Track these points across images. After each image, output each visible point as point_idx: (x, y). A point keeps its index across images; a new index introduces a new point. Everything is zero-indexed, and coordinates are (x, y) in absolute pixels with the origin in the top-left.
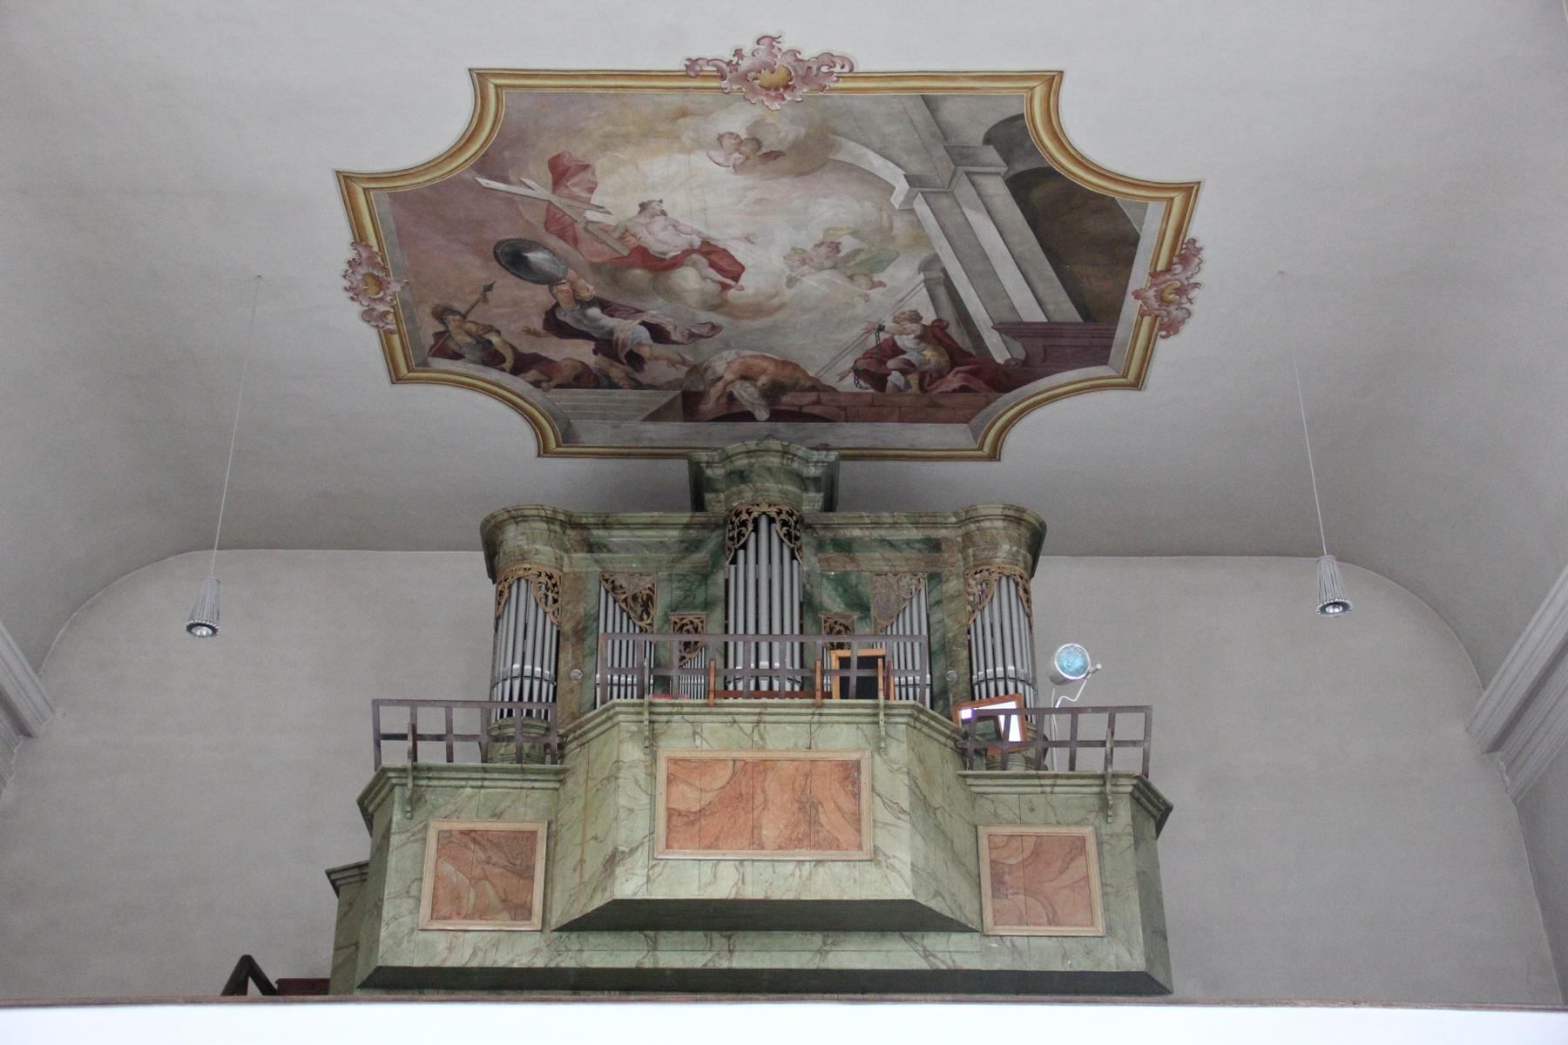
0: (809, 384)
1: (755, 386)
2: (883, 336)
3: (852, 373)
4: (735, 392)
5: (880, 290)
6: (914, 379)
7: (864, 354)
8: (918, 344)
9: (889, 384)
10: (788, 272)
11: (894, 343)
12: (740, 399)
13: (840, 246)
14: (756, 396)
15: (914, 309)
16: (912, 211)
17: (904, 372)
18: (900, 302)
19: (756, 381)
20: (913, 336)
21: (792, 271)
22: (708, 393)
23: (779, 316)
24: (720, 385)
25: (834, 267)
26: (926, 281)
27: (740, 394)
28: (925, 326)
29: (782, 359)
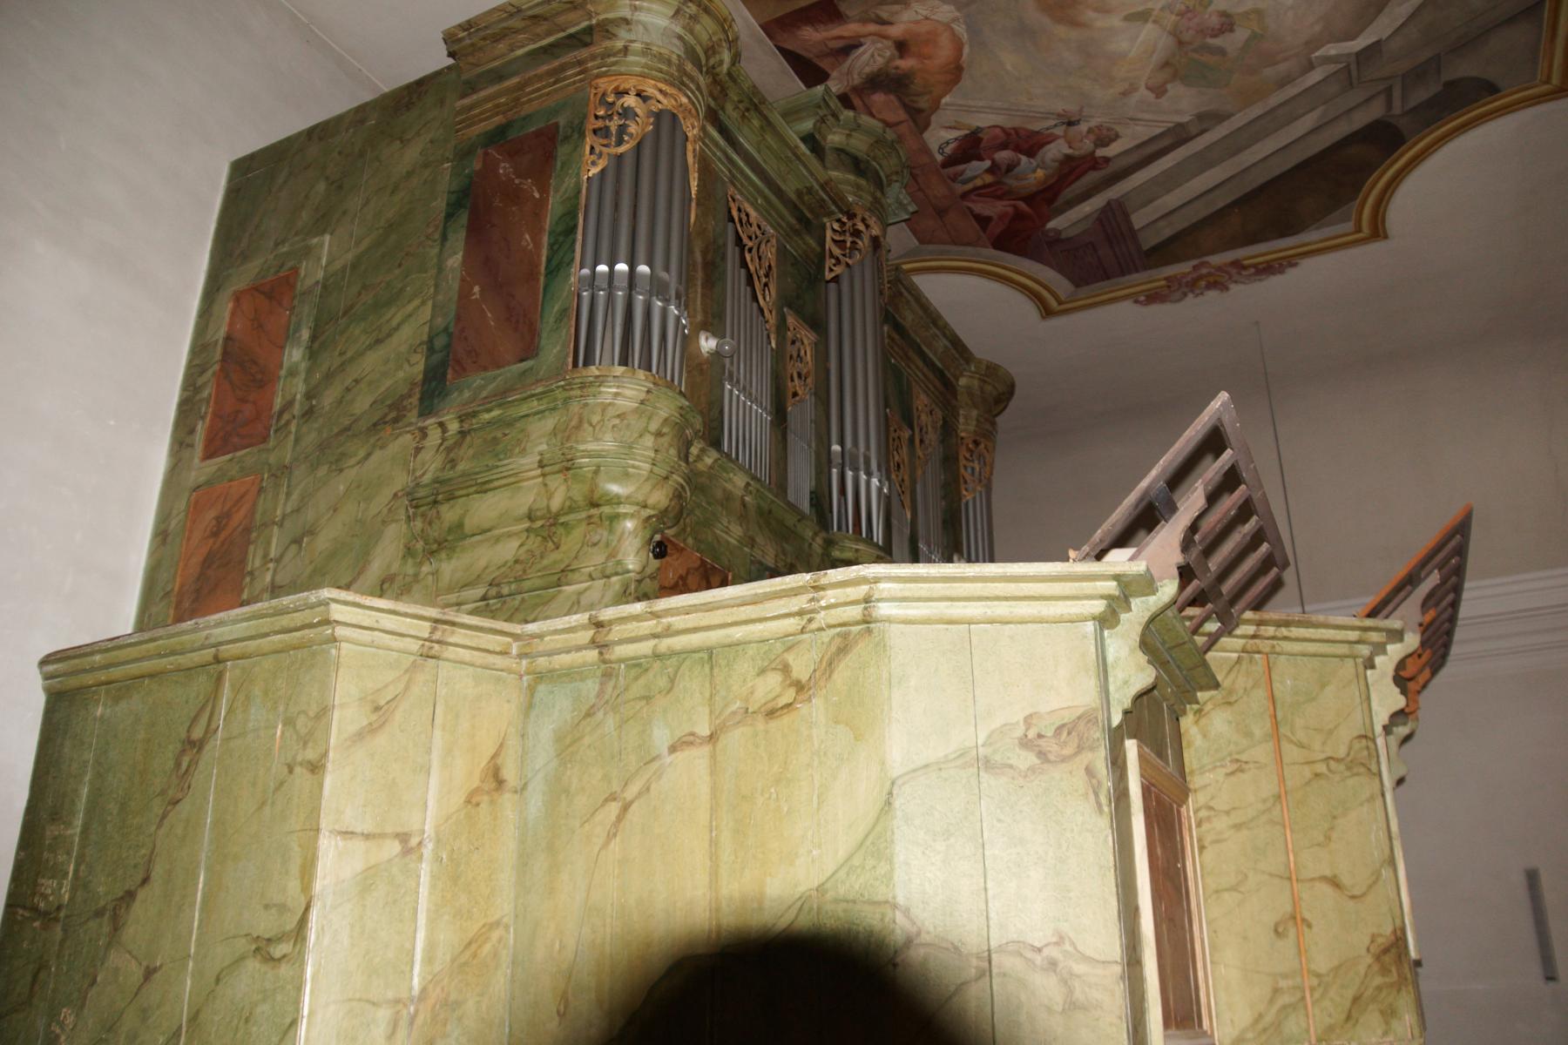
0: (923, 103)
1: (891, 59)
2: (1059, 131)
3: (968, 132)
4: (861, 49)
5: (1150, 96)
6: (989, 179)
7: (1014, 129)
8: (1053, 161)
9: (961, 167)
10: (1159, 6)
11: (1049, 143)
12: (852, 57)
13: (1227, 34)
14: (867, 70)
15: (1120, 134)
16: (1311, 66)
17: (990, 171)
18: (1131, 119)
19: (901, 57)
20: (1069, 151)
21: (1162, 9)
22: (846, 22)
23: (1061, 31)
24: (872, 28)
25: (1180, 43)
26: (1180, 125)
27: (864, 53)
28: (1094, 152)
29: (965, 65)
